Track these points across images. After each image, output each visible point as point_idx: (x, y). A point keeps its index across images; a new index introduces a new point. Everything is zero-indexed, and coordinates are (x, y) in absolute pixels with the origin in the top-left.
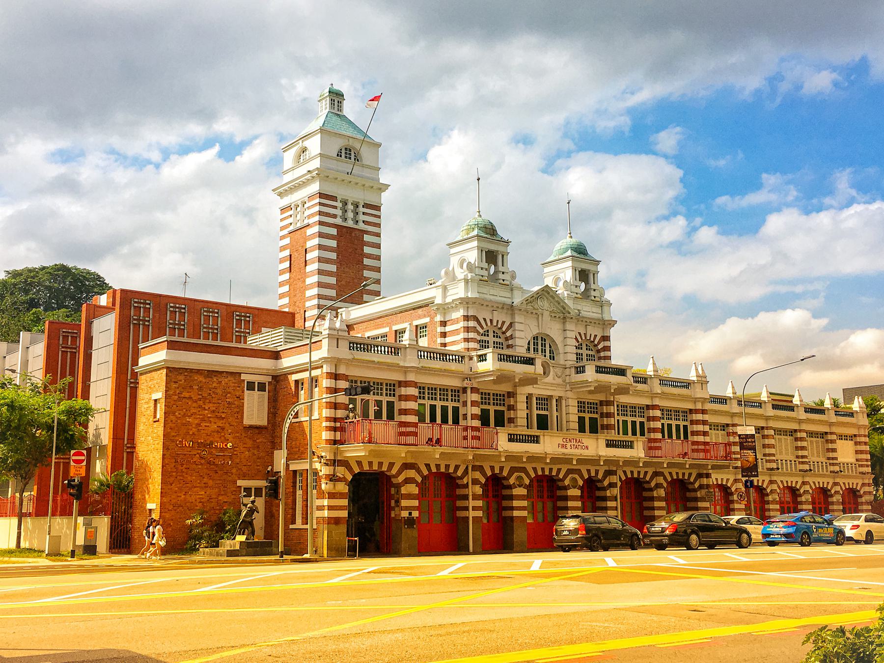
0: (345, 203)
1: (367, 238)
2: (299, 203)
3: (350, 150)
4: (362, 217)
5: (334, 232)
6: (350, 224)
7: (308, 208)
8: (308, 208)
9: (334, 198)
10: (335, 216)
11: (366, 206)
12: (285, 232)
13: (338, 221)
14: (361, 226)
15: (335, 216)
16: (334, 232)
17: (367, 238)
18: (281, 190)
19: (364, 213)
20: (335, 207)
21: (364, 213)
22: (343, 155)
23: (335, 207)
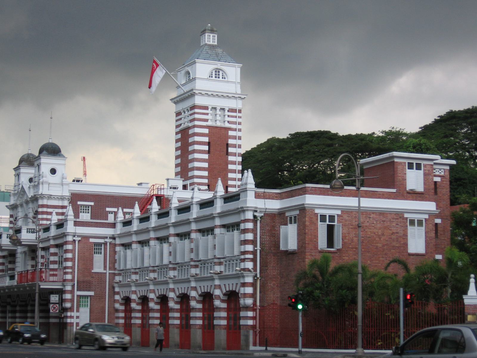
1: (231, 133)
4: (227, 119)
5: (206, 131)
6: (219, 124)
9: (206, 108)
10: (207, 120)
12: (178, 130)
13: (209, 123)
14: (227, 125)
15: (207, 120)
16: (206, 131)
17: (231, 133)
18: (175, 100)
19: (228, 116)
20: (207, 114)
21: (228, 116)
22: (214, 76)
23: (207, 114)
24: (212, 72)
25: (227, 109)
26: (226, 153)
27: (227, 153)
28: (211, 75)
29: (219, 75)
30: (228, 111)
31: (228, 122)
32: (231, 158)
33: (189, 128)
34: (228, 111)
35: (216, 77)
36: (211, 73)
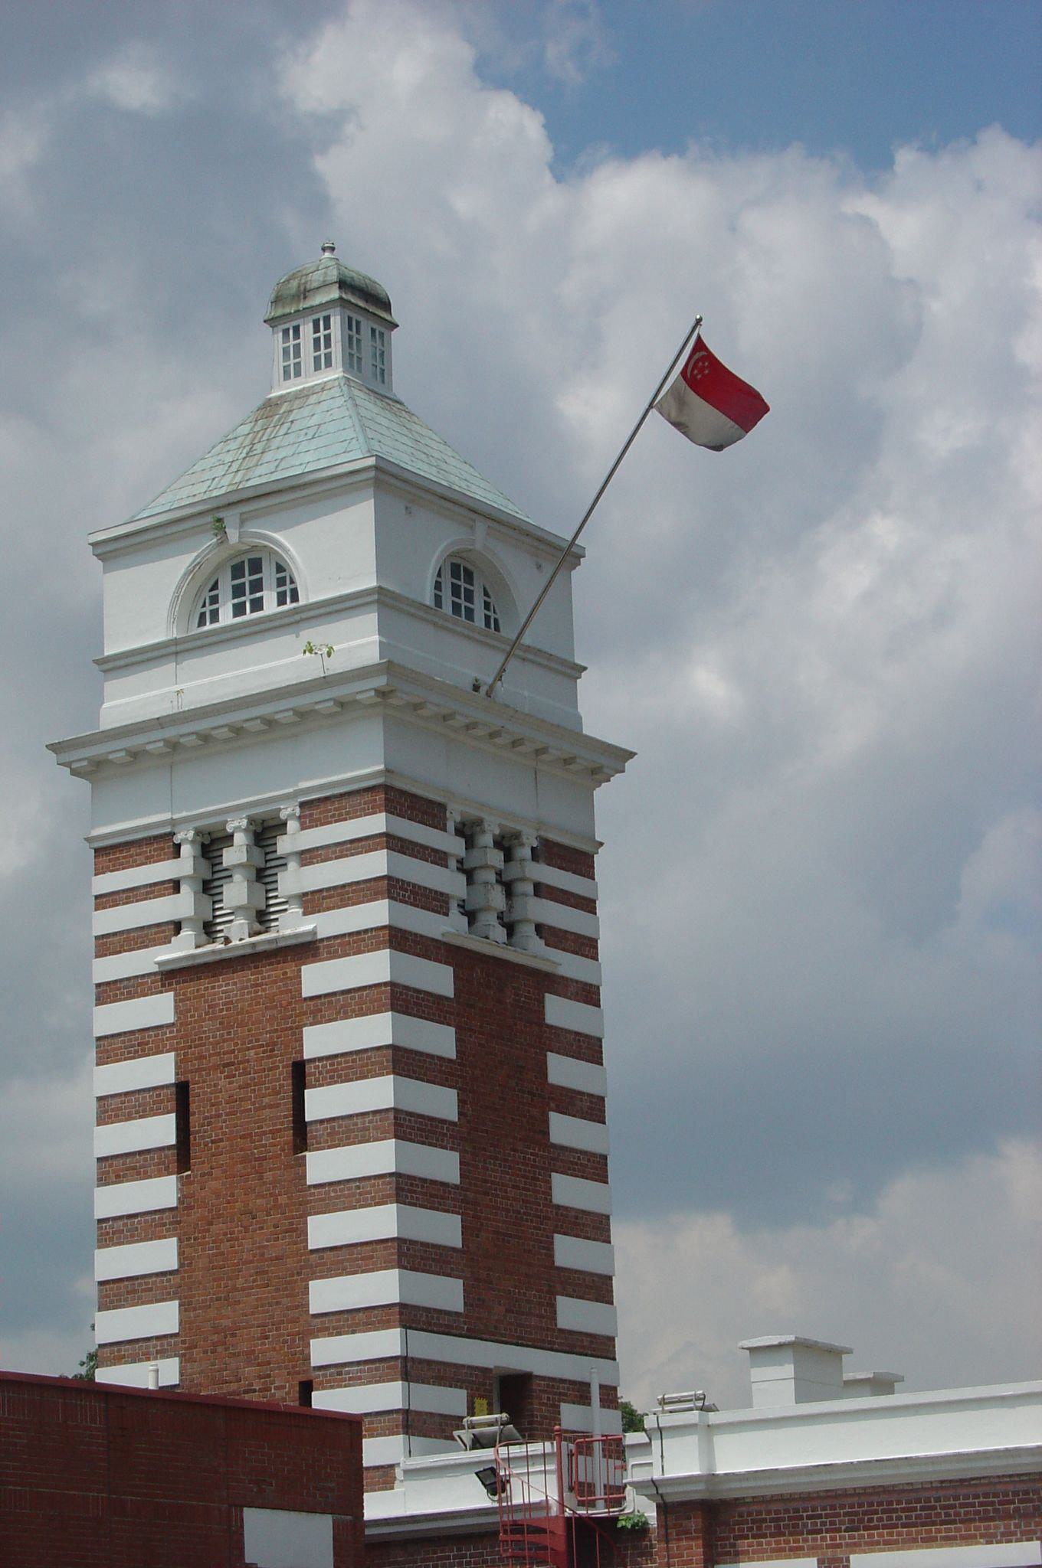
0: (468, 831)
2: (237, 825)
3: (256, 566)
5: (439, 979)
7: (308, 857)
8: (308, 857)
9: (429, 812)
10: (436, 902)
11: (551, 852)
16: (439, 979)
17: (559, 1012)
22: (448, 599)
23: (438, 858)
24: (215, 587)
25: (530, 840)
26: (288, 1136)
27: (302, 1135)
28: (208, 608)
29: (469, 597)
30: (535, 855)
31: (540, 929)
32: (323, 1166)
33: (308, 949)
34: (535, 855)
35: (456, 608)
36: (207, 595)
